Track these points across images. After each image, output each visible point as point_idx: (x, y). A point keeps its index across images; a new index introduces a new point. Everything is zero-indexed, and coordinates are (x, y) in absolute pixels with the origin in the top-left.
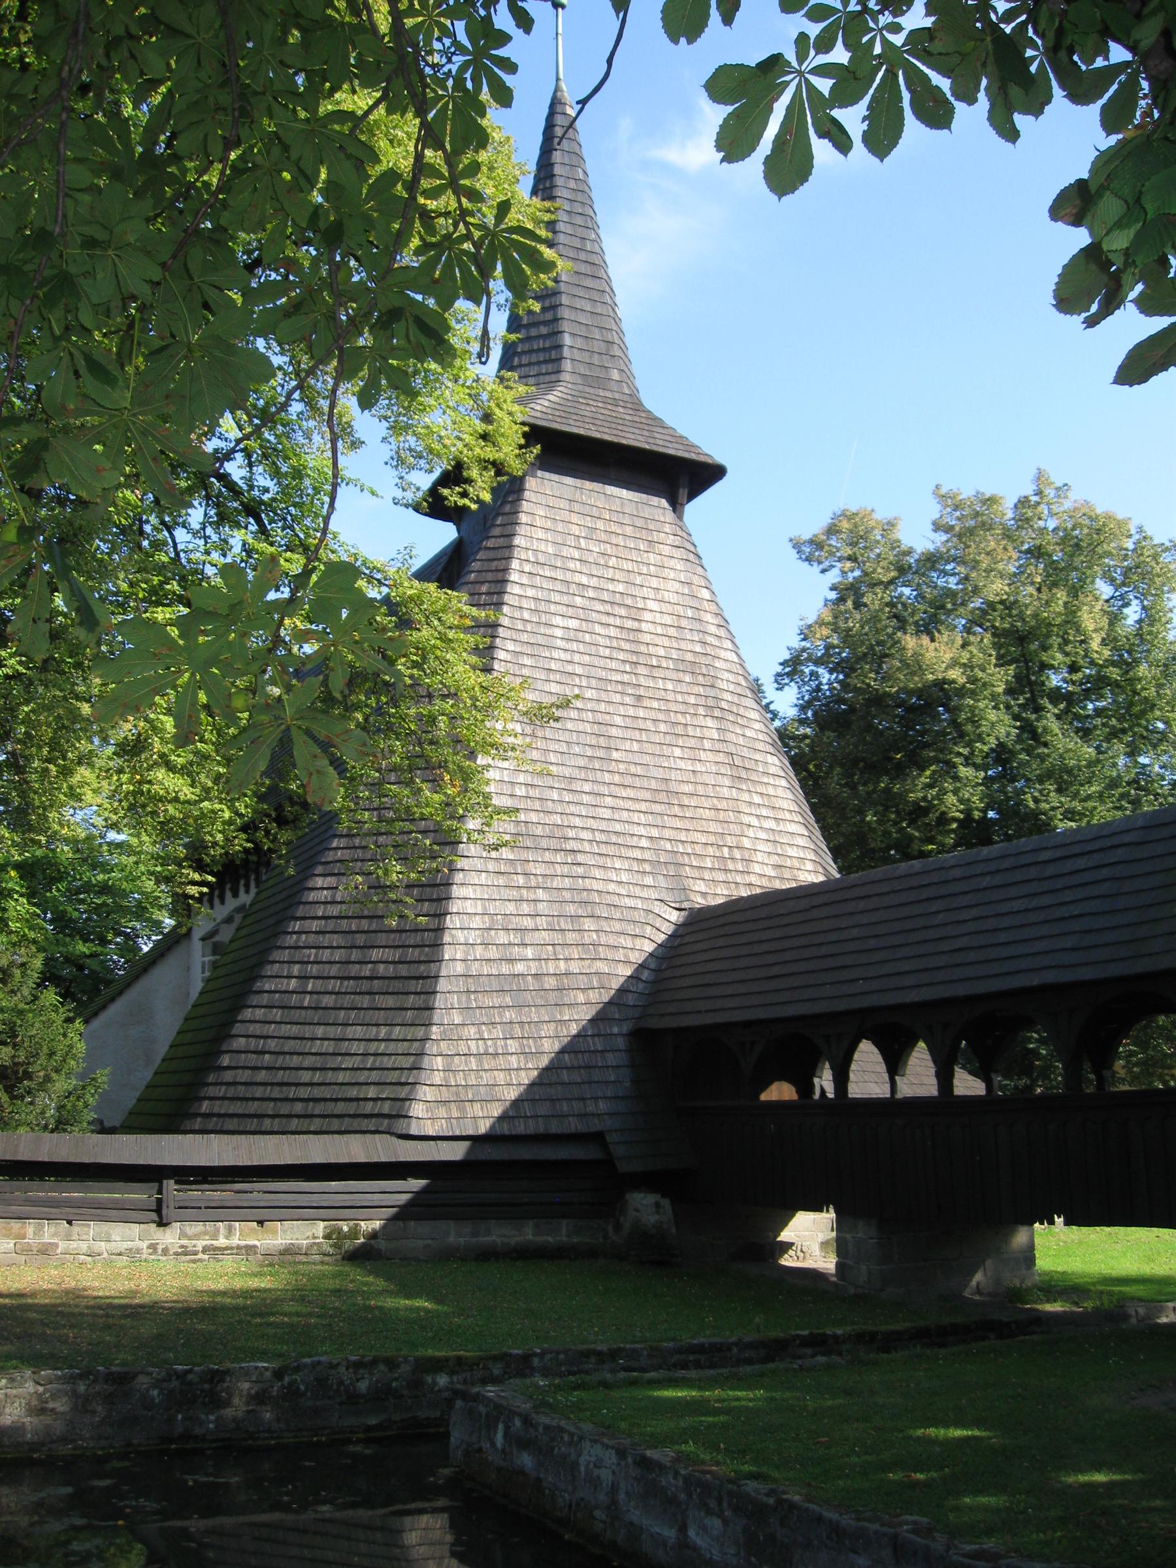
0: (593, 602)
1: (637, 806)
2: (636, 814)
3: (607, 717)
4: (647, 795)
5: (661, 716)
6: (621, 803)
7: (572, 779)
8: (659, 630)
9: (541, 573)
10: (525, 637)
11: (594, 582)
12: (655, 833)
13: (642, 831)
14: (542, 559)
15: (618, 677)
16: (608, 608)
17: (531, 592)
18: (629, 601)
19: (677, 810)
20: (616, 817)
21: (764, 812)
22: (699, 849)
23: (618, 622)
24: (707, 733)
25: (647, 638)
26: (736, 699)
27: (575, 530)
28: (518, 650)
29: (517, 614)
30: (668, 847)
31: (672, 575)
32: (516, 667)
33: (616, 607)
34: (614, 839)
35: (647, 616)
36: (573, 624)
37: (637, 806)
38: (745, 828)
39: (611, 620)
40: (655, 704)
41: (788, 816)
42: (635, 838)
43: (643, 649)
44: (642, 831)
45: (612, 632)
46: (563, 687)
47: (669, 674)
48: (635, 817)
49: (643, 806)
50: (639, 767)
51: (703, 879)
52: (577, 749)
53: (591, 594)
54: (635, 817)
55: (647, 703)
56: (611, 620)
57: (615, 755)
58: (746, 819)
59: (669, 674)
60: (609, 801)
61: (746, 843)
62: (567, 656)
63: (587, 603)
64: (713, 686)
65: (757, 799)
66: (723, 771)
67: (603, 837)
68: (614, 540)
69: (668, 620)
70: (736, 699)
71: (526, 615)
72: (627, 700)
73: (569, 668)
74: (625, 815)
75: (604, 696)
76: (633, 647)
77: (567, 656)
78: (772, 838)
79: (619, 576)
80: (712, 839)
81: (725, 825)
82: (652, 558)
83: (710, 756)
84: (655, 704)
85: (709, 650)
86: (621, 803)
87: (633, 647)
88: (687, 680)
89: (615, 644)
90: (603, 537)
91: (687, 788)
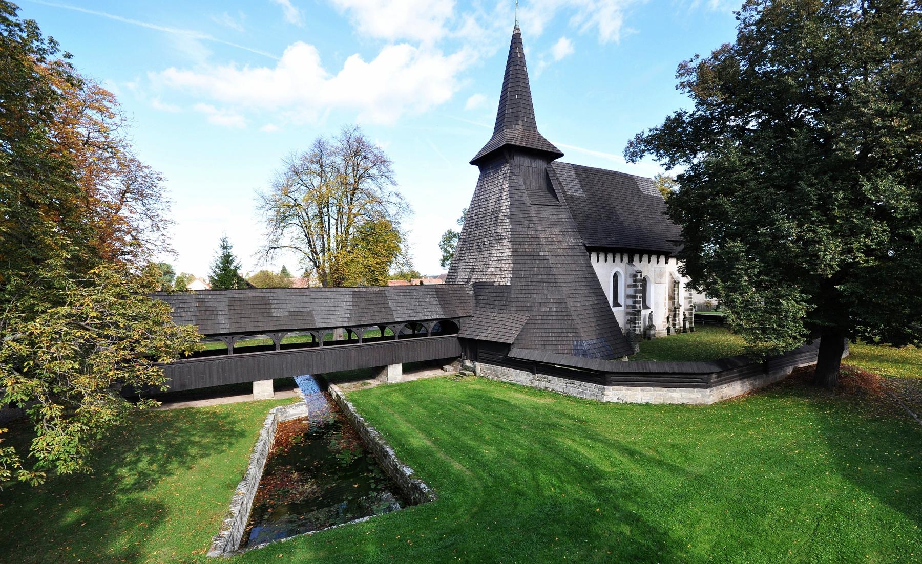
19: (480, 257)
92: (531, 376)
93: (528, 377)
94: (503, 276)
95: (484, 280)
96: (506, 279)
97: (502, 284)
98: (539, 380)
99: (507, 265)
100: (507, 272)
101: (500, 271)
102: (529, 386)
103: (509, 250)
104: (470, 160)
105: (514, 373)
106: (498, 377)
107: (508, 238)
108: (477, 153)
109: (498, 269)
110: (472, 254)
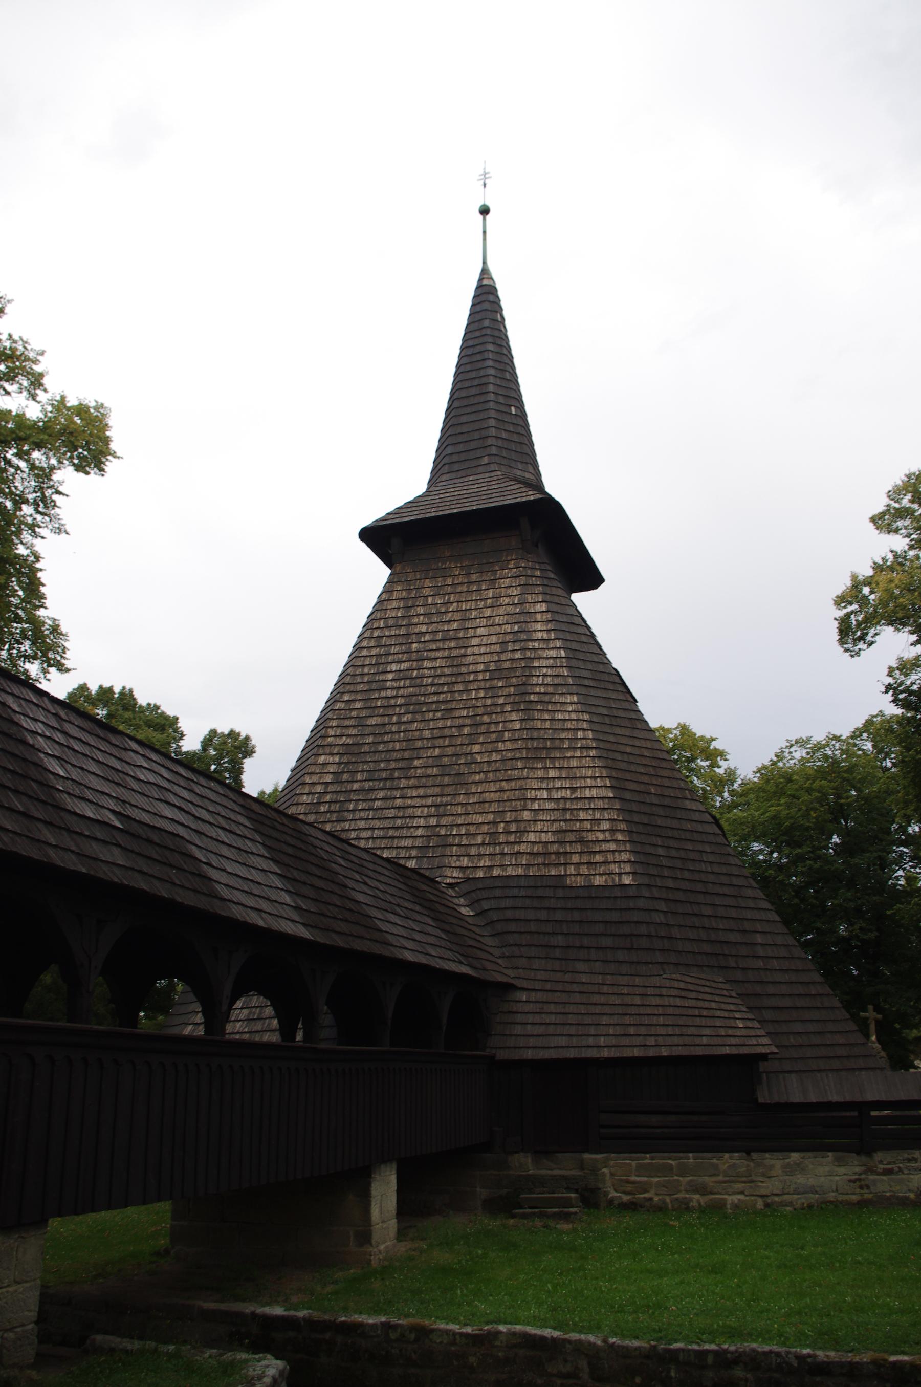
0: (427, 644)
1: (424, 802)
2: (420, 810)
3: (417, 733)
4: (437, 790)
5: (468, 721)
6: (409, 802)
7: (372, 790)
8: (483, 650)
9: (387, 633)
10: (361, 687)
11: (432, 628)
12: (433, 821)
13: (422, 822)
14: (391, 622)
15: (435, 699)
16: (440, 645)
17: (374, 652)
18: (461, 634)
19: (462, 799)
20: (401, 814)
21: (558, 784)
22: (472, 829)
23: (446, 653)
24: (510, 726)
25: (470, 659)
26: (550, 690)
27: (426, 592)
28: (352, 698)
29: (359, 671)
30: (443, 832)
31: (507, 600)
32: (348, 712)
33: (447, 643)
34: (391, 833)
35: (475, 641)
36: (404, 666)
37: (424, 802)
38: (529, 802)
39: (438, 654)
40: (465, 713)
41: (589, 782)
42: (412, 830)
43: (464, 669)
44: (422, 822)
45: (438, 663)
46: (383, 718)
47: (482, 684)
48: (418, 812)
49: (429, 801)
50: (435, 769)
51: (469, 855)
52: (382, 765)
53: (427, 638)
54: (418, 812)
55: (457, 713)
56: (438, 654)
57: (416, 763)
58: (530, 794)
59: (482, 684)
60: (399, 802)
61: (526, 815)
62: (394, 693)
63: (421, 646)
64: (524, 684)
65: (552, 773)
66: (518, 756)
67: (381, 833)
68: (459, 589)
69: (494, 639)
70: (550, 690)
71: (366, 670)
72: (439, 715)
73: (392, 702)
74: (410, 811)
75: (419, 717)
76: (455, 670)
77: (394, 693)
78: (561, 806)
79: (457, 616)
80: (491, 817)
81: (508, 803)
82: (490, 593)
83: (509, 745)
84: (465, 713)
85: (528, 654)
86: (409, 802)
87: (455, 670)
88: (500, 684)
89: (439, 672)
90: (449, 589)
91: (477, 778)
92: (853, 1167)
93: (842, 1170)
94: (598, 858)
95: (510, 871)
96: (615, 868)
97: (598, 881)
98: (889, 1172)
99: (605, 825)
100: (612, 846)
101: (581, 841)
102: (855, 1198)
103: (599, 782)
104: (367, 521)
105: (778, 1164)
106: (703, 1190)
107: (589, 748)
108: (391, 508)
109: (571, 837)
110: (410, 793)
